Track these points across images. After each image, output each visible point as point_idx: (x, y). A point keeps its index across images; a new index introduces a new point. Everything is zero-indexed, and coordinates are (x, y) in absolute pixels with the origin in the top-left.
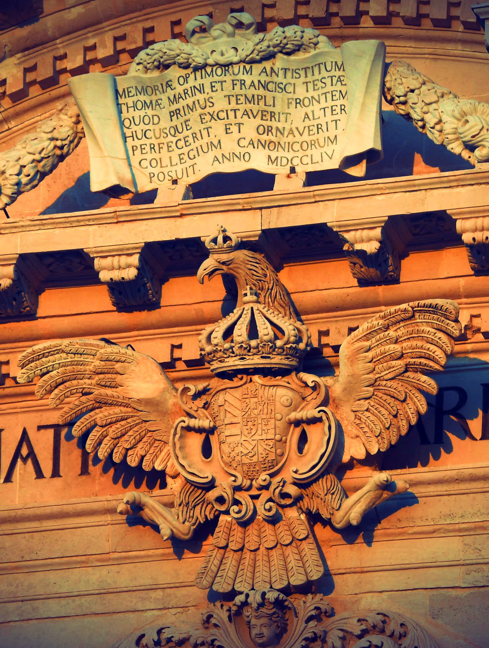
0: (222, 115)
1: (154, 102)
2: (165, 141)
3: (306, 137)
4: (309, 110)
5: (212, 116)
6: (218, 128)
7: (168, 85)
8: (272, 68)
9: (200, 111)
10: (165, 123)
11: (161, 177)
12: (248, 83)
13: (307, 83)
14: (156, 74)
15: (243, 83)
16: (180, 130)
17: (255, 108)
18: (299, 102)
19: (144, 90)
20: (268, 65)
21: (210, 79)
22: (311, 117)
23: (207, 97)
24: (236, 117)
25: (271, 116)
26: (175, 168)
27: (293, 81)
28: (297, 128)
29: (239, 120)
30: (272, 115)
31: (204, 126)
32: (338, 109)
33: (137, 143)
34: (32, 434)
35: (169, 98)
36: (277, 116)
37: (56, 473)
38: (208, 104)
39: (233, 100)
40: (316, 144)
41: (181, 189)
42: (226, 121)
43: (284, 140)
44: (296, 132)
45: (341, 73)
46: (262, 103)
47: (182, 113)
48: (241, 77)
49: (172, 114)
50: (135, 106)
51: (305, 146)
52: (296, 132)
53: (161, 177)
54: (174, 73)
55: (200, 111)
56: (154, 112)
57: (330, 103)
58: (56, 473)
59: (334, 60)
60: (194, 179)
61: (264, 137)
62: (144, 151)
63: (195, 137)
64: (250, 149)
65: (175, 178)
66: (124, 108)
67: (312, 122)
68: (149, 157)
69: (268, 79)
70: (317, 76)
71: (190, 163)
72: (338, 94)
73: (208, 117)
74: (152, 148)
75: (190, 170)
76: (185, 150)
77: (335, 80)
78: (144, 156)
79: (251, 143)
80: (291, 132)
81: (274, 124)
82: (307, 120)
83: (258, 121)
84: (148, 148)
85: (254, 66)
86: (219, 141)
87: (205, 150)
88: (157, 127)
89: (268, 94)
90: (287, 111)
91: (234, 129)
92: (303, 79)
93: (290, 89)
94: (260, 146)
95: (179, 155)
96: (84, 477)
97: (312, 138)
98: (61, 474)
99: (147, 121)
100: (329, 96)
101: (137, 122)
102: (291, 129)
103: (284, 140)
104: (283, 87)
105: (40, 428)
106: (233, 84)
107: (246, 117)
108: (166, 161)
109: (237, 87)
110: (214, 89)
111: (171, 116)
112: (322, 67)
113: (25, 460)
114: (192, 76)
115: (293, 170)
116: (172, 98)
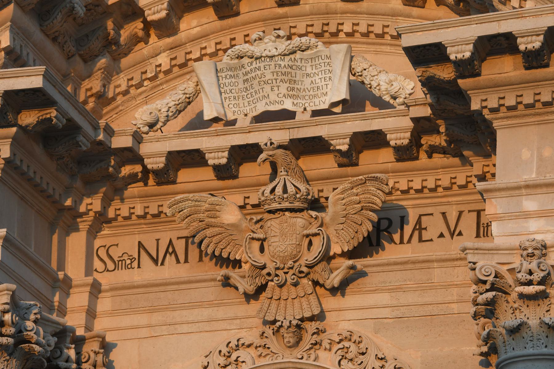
0: (270, 82)
1: (235, 75)
2: (241, 95)
3: (311, 93)
4: (313, 79)
5: (264, 82)
6: (267, 88)
7: (243, 66)
8: (295, 58)
9: (258, 79)
10: (241, 86)
11: (239, 112)
12: (283, 66)
13: (312, 65)
14: (236, 61)
15: (280, 66)
16: (249, 89)
17: (286, 78)
18: (308, 75)
19: (230, 69)
20: (292, 56)
21: (264, 64)
22: (314, 82)
23: (262, 72)
24: (276, 83)
25: (294, 82)
26: (246, 108)
27: (305, 65)
28: (307, 88)
29: (278, 84)
30: (295, 81)
31: (260, 87)
32: (328, 79)
33: (227, 96)
34: (175, 241)
35: (243, 73)
36: (297, 82)
37: (186, 261)
38: (263, 76)
39: (275, 74)
40: (317, 96)
41: (249, 119)
42: (272, 85)
43: (301, 94)
44: (307, 90)
45: (329, 61)
46: (289, 75)
47: (250, 80)
48: (279, 62)
49: (245, 81)
50: (226, 77)
51: (311, 97)
52: (307, 90)
53: (239, 112)
54: (246, 60)
55: (258, 79)
56: (235, 80)
57: (324, 76)
58: (186, 261)
59: (326, 54)
60: (255, 114)
61: (291, 93)
62: (230, 100)
63: (256, 93)
64: (284, 99)
65: (246, 113)
66: (220, 78)
67: (314, 86)
68: (233, 102)
69: (292, 64)
70: (317, 62)
71: (253, 106)
72: (328, 71)
73: (262, 83)
74: (235, 98)
75: (254, 109)
76: (251, 99)
77: (326, 64)
78: (231, 102)
79: (284, 96)
80: (304, 90)
81: (296, 86)
82: (312, 84)
83: (287, 85)
84: (232, 98)
85: (286, 57)
86: (268, 95)
87: (261, 99)
88: (237, 88)
89: (293, 71)
90: (302, 80)
91: (276, 89)
92: (310, 64)
93: (304, 68)
94: (289, 97)
95: (248, 102)
96: (200, 263)
97: (315, 93)
98: (189, 261)
99: (232, 85)
100: (323, 72)
101: (227, 85)
102: (304, 89)
103: (301, 94)
104: (300, 67)
105: (178, 238)
106: (275, 66)
107: (281, 83)
108: (241, 105)
109: (277, 68)
110: (266, 69)
111: (244, 82)
112: (320, 57)
113: (171, 254)
114: (255, 62)
115: (305, 109)
116: (244, 73)
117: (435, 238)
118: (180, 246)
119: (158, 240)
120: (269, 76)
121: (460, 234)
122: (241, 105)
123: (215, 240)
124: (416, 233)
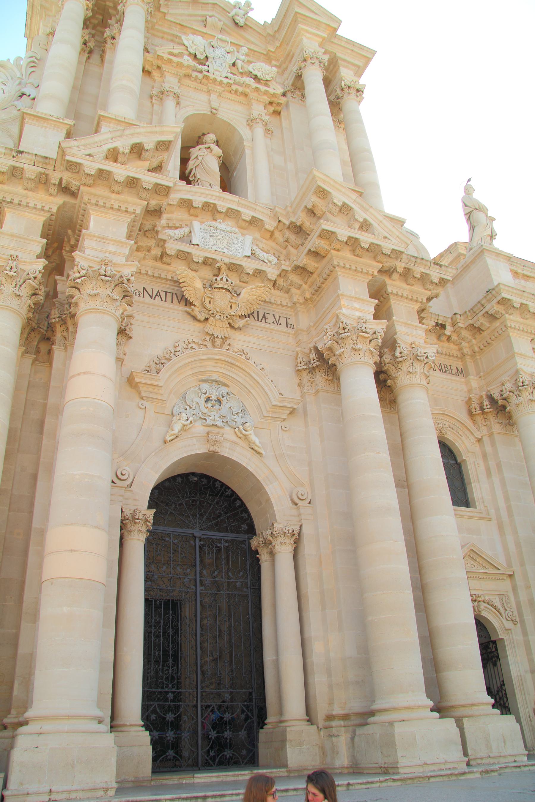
6: (219, 242)
10: (207, 237)
19: (205, 230)
37: (166, 301)
54: (212, 228)
58: (166, 301)
63: (213, 242)
103: (231, 249)
108: (205, 245)
117: (271, 323)
118: (163, 295)
119: (152, 289)
120: (220, 237)
121: (280, 324)
122: (205, 245)
123: (190, 293)
124: (264, 319)
